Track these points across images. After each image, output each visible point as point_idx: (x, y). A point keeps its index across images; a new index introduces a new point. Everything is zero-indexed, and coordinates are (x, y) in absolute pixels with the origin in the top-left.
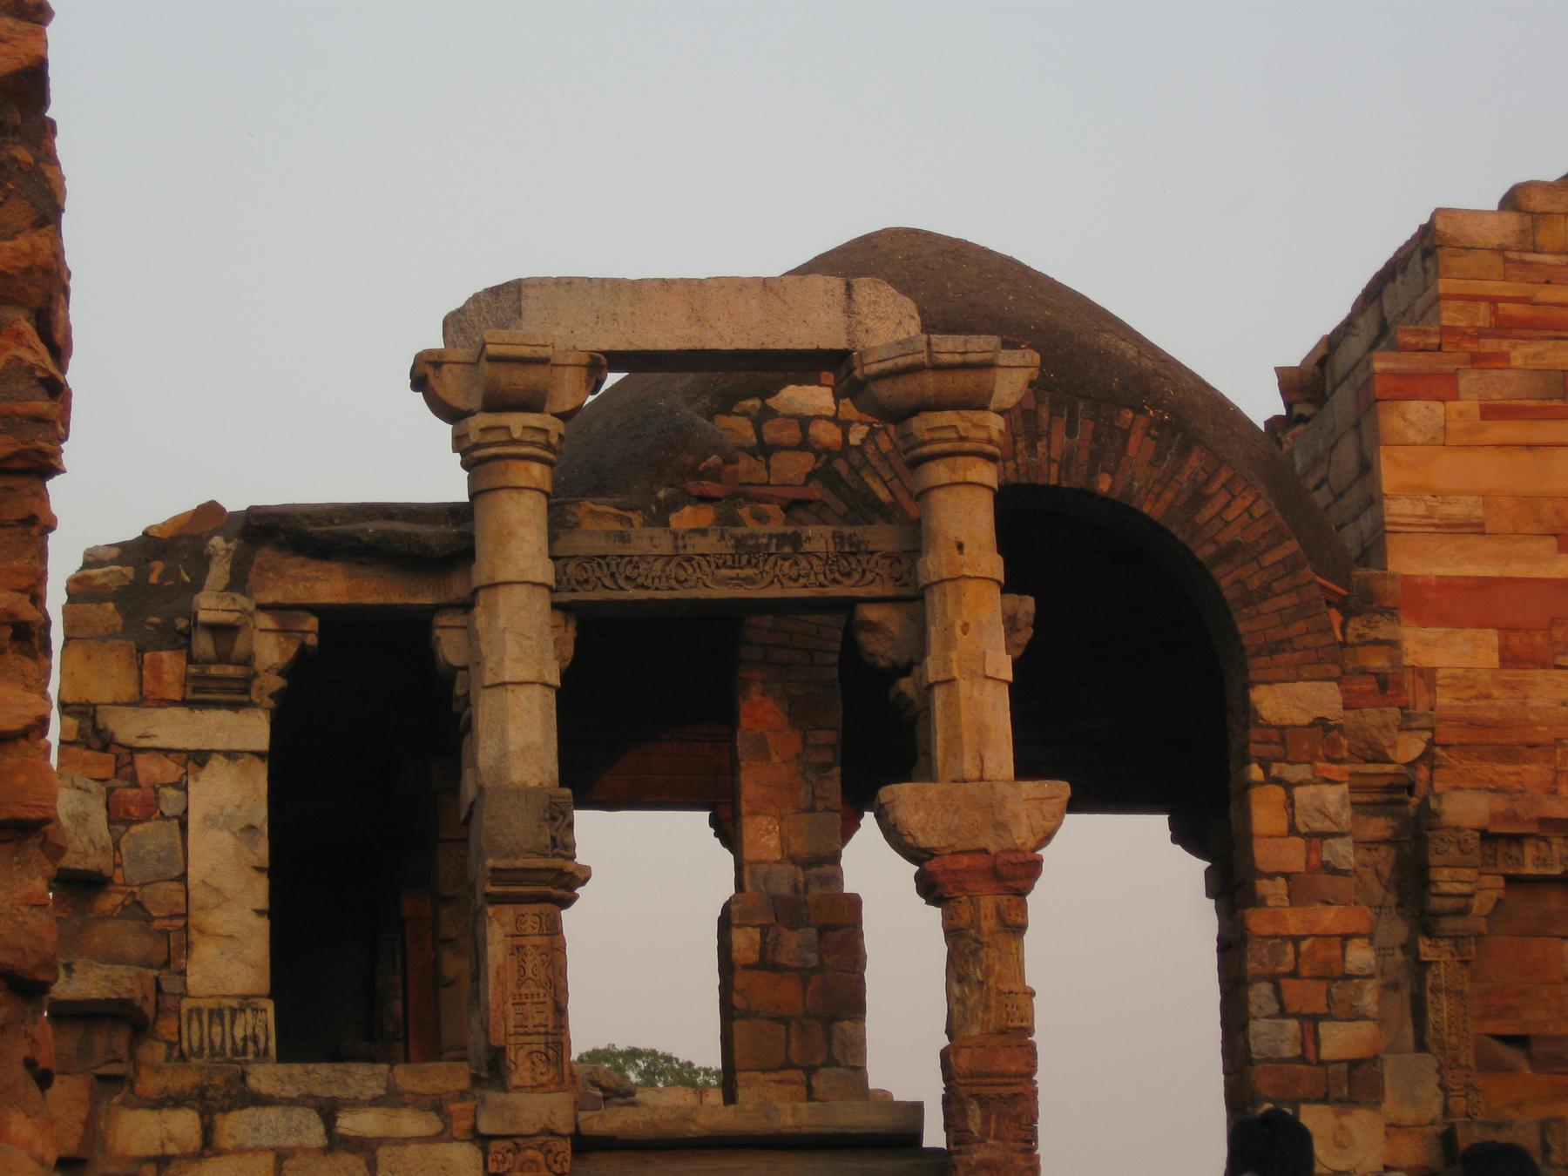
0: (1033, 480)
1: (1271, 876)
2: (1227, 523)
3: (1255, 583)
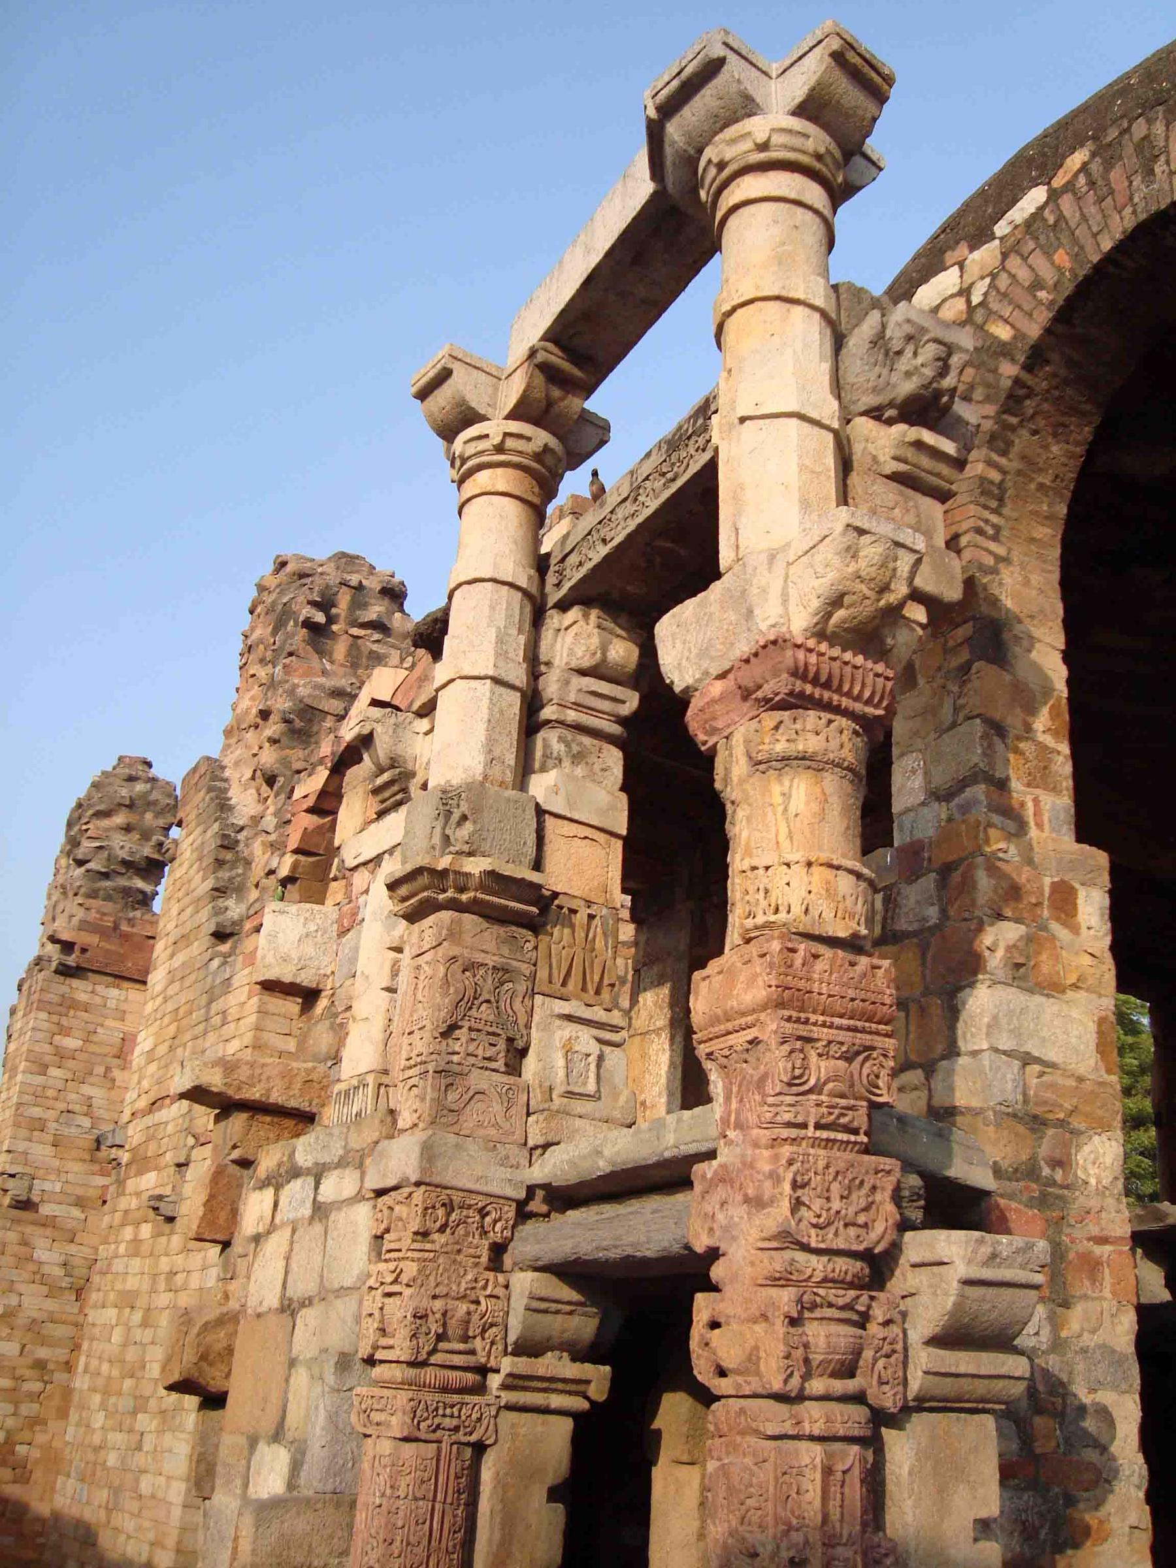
0: (1154, 209)
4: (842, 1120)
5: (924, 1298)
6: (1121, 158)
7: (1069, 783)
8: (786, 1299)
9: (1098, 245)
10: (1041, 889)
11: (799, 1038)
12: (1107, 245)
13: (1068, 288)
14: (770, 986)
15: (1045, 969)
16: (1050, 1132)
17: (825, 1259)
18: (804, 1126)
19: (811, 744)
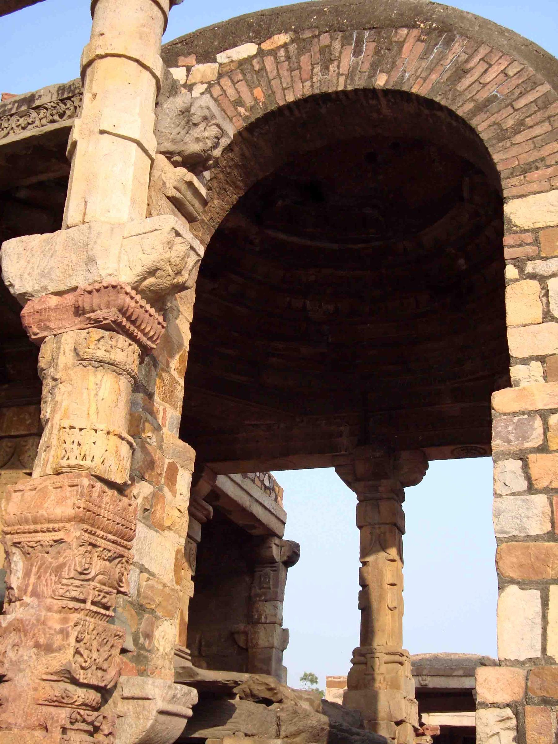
0: (324, 90)
1: (525, 361)
2: (485, 85)
3: (510, 122)
4: (104, 601)
5: (130, 720)
6: (310, 51)
7: (180, 404)
8: (63, 716)
9: (285, 96)
10: (163, 465)
11: (91, 544)
12: (290, 98)
13: (259, 114)
14: (79, 508)
15: (158, 515)
16: (146, 616)
17: (84, 690)
18: (84, 601)
19: (119, 356)
